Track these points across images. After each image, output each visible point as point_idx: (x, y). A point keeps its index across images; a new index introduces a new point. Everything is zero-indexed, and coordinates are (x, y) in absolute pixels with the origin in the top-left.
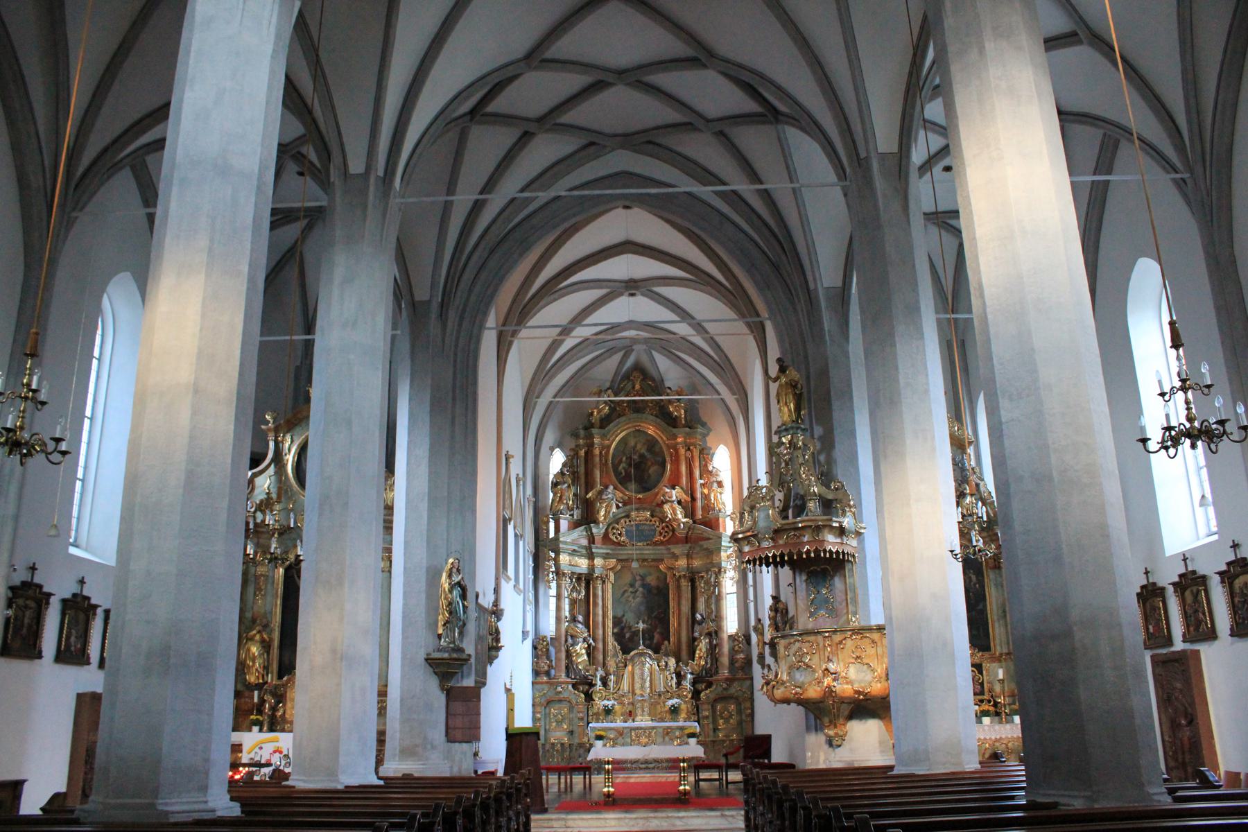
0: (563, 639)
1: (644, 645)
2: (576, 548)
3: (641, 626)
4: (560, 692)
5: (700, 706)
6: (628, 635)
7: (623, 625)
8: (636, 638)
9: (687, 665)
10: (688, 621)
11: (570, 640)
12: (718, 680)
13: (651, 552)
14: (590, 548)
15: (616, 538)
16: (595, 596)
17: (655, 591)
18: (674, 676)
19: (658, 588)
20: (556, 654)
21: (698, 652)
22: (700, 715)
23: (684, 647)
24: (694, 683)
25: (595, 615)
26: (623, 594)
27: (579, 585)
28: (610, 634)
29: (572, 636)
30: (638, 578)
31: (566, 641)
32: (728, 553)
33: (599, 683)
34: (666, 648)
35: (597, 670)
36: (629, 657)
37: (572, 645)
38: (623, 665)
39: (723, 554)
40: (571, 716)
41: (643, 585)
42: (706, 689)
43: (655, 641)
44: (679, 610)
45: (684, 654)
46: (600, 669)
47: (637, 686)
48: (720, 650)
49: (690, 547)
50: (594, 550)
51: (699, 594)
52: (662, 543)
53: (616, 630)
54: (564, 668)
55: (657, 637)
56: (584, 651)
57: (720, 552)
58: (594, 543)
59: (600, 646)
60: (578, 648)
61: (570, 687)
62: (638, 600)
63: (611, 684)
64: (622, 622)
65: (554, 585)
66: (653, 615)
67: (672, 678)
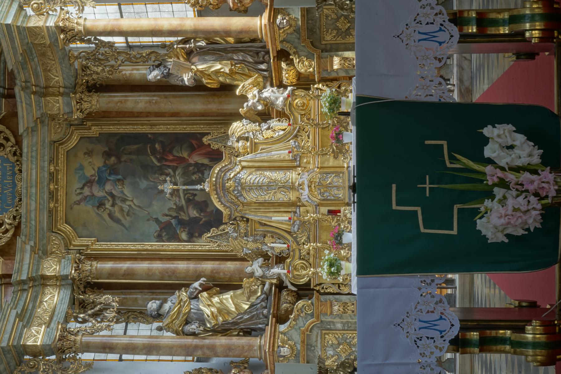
0: (190, 341)
1: (201, 181)
2: (14, 313)
3: (168, 187)
4: (292, 348)
5: (325, 75)
6: (194, 213)
7: (173, 222)
8: (197, 198)
9: (244, 98)
10: (166, 97)
11: (193, 327)
12: (273, 39)
13: (34, 166)
14: (23, 282)
15: (7, 231)
16: (112, 274)
17: (113, 159)
18: (264, 126)
19: (107, 155)
20: (218, 356)
21: (221, 79)
22: (342, 74)
23: (213, 105)
24: (281, 86)
25: (149, 276)
26: (118, 221)
27: (94, 304)
28: (188, 246)
29: (187, 322)
30: (86, 191)
31: (194, 334)
32: (32, 13)
33: (276, 270)
34: (215, 140)
35: (251, 275)
36: (225, 212)
37: (202, 321)
38: (242, 225)
39: (35, 22)
40: (339, 326)
41: (101, 182)
42: (290, 63)
43: (206, 161)
44: (148, 114)
45: (228, 107)
46: (249, 270)
47: (281, 197)
48: (216, 32)
49: (24, 89)
50: (24, 277)
51: (116, 76)
52: (18, 143)
53: (184, 236)
54: (244, 341)
55: (196, 158)
56: (216, 299)
57: (30, 29)
58: (10, 276)
59: (208, 266)
60: (207, 311)
61: (282, 328)
62: (127, 192)
63: (280, 246)
64: (169, 224)
65: (87, 356)
66: (158, 164)
67: (268, 128)
